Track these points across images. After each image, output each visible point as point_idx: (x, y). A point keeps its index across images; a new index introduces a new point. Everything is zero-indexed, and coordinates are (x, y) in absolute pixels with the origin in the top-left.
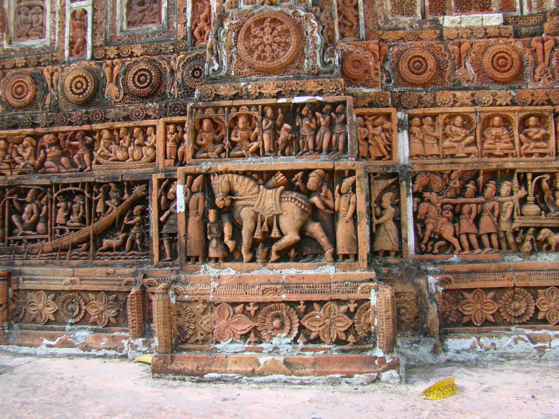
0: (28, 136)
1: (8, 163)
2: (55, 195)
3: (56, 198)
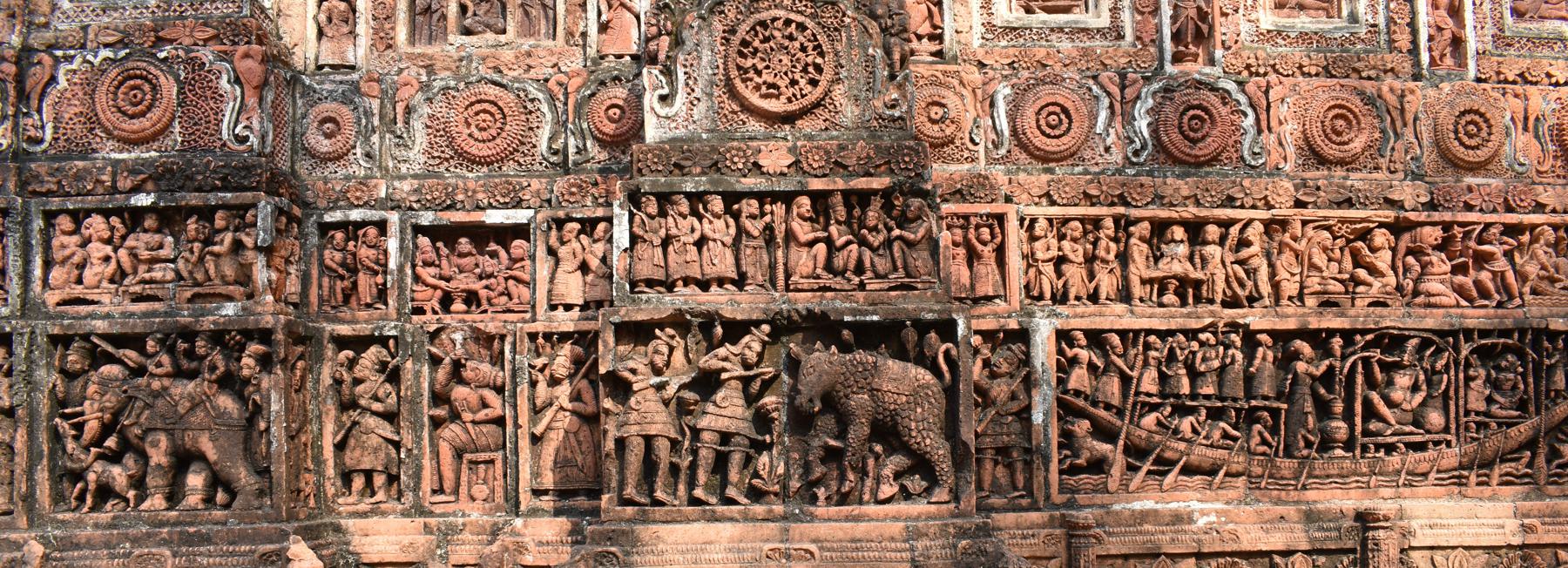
0: (1381, 225)
1: (1341, 281)
2: (1464, 353)
3: (1466, 358)
